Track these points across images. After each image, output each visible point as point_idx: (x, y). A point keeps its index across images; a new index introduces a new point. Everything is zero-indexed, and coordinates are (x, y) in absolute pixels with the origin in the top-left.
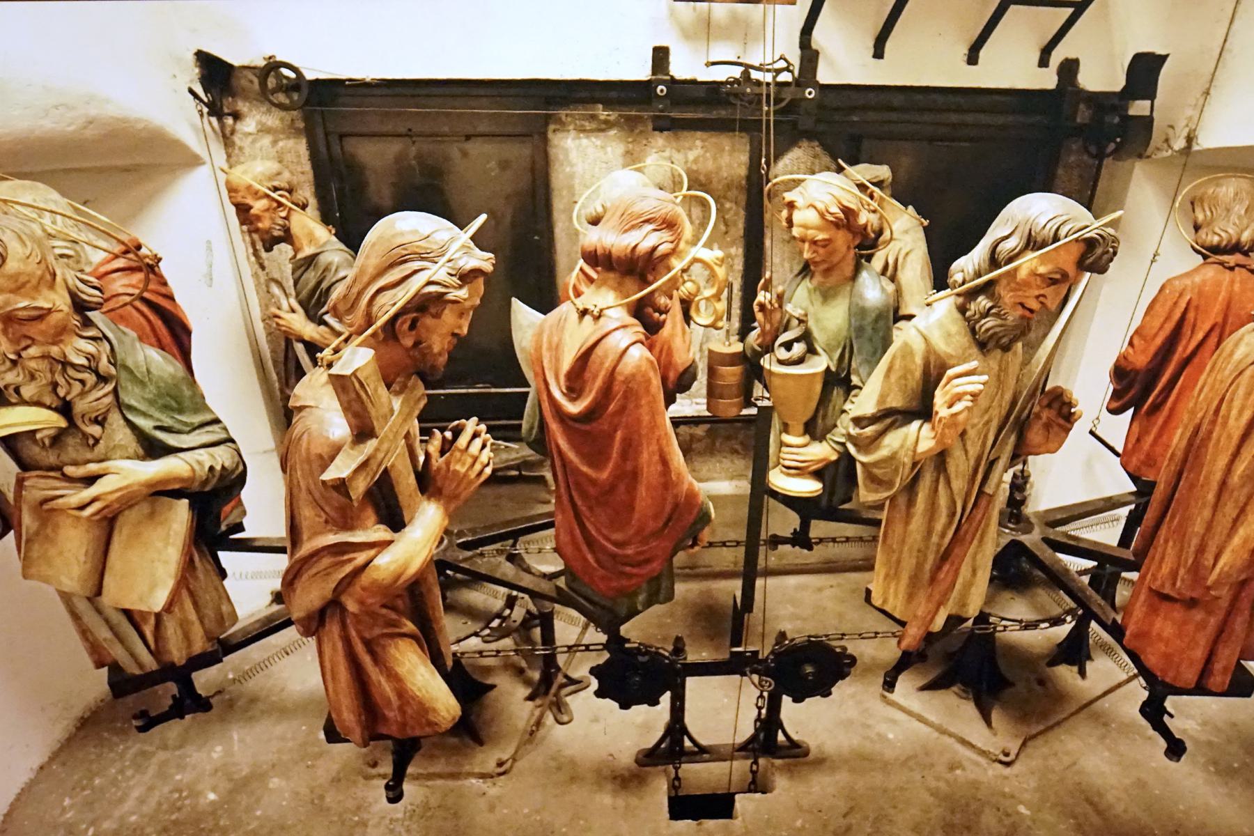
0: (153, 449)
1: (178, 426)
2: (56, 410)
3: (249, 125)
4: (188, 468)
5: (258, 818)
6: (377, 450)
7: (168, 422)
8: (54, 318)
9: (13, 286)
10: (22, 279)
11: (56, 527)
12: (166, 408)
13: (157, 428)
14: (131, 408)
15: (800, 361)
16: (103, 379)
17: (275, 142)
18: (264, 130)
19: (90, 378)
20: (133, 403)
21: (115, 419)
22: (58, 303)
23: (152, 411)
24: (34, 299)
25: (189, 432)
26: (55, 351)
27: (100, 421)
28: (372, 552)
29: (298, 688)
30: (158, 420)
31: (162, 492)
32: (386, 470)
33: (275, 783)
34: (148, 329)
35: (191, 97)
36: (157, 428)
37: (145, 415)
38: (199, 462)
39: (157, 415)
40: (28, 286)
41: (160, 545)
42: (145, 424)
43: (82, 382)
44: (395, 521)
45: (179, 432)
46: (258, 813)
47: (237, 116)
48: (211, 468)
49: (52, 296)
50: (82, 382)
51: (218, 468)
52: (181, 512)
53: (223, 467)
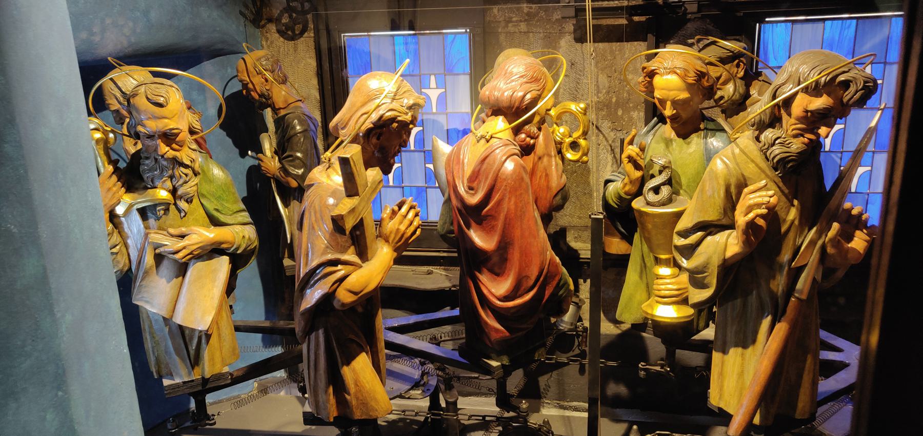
0: (215, 222)
2: (169, 191)
6: (359, 204)
14: (203, 196)
15: (669, 201)
16: (196, 174)
21: (195, 201)
27: (189, 201)
28: (350, 268)
31: (214, 251)
32: (362, 219)
42: (210, 207)
43: (186, 175)
44: (363, 254)
50: (186, 175)
52: (223, 264)
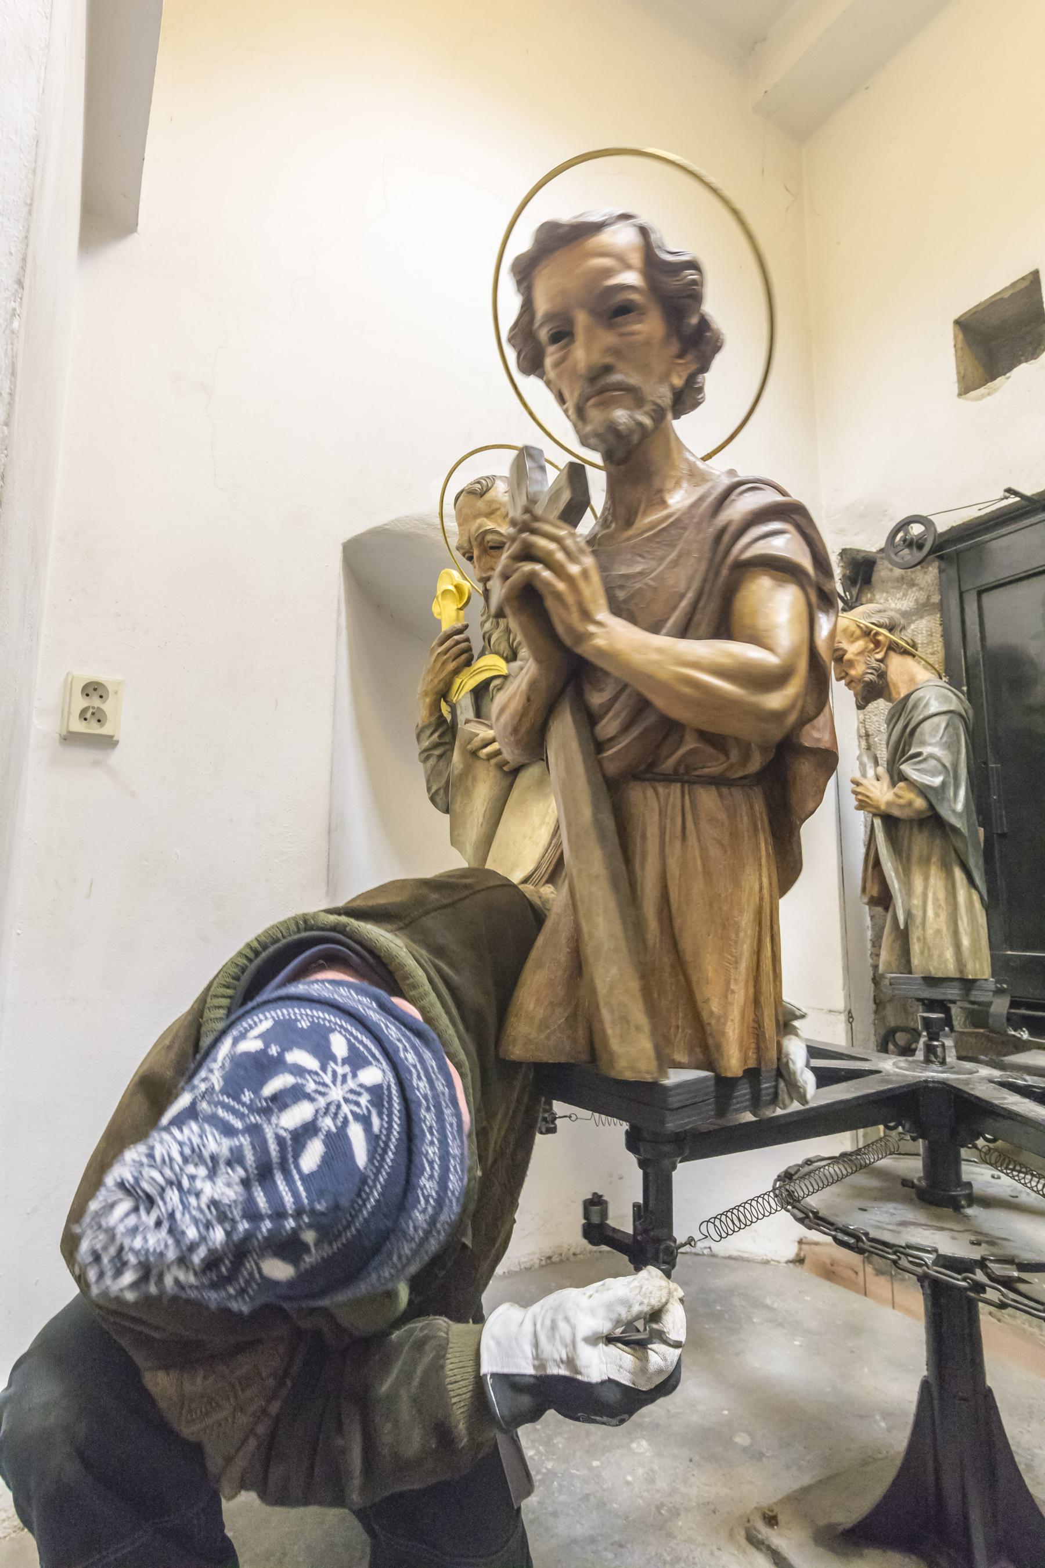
5: (590, 1468)
9: (487, 511)
10: (495, 506)
11: (474, 779)
24: (499, 525)
29: (757, 1365)
40: (498, 513)
41: (536, 820)
46: (596, 1463)
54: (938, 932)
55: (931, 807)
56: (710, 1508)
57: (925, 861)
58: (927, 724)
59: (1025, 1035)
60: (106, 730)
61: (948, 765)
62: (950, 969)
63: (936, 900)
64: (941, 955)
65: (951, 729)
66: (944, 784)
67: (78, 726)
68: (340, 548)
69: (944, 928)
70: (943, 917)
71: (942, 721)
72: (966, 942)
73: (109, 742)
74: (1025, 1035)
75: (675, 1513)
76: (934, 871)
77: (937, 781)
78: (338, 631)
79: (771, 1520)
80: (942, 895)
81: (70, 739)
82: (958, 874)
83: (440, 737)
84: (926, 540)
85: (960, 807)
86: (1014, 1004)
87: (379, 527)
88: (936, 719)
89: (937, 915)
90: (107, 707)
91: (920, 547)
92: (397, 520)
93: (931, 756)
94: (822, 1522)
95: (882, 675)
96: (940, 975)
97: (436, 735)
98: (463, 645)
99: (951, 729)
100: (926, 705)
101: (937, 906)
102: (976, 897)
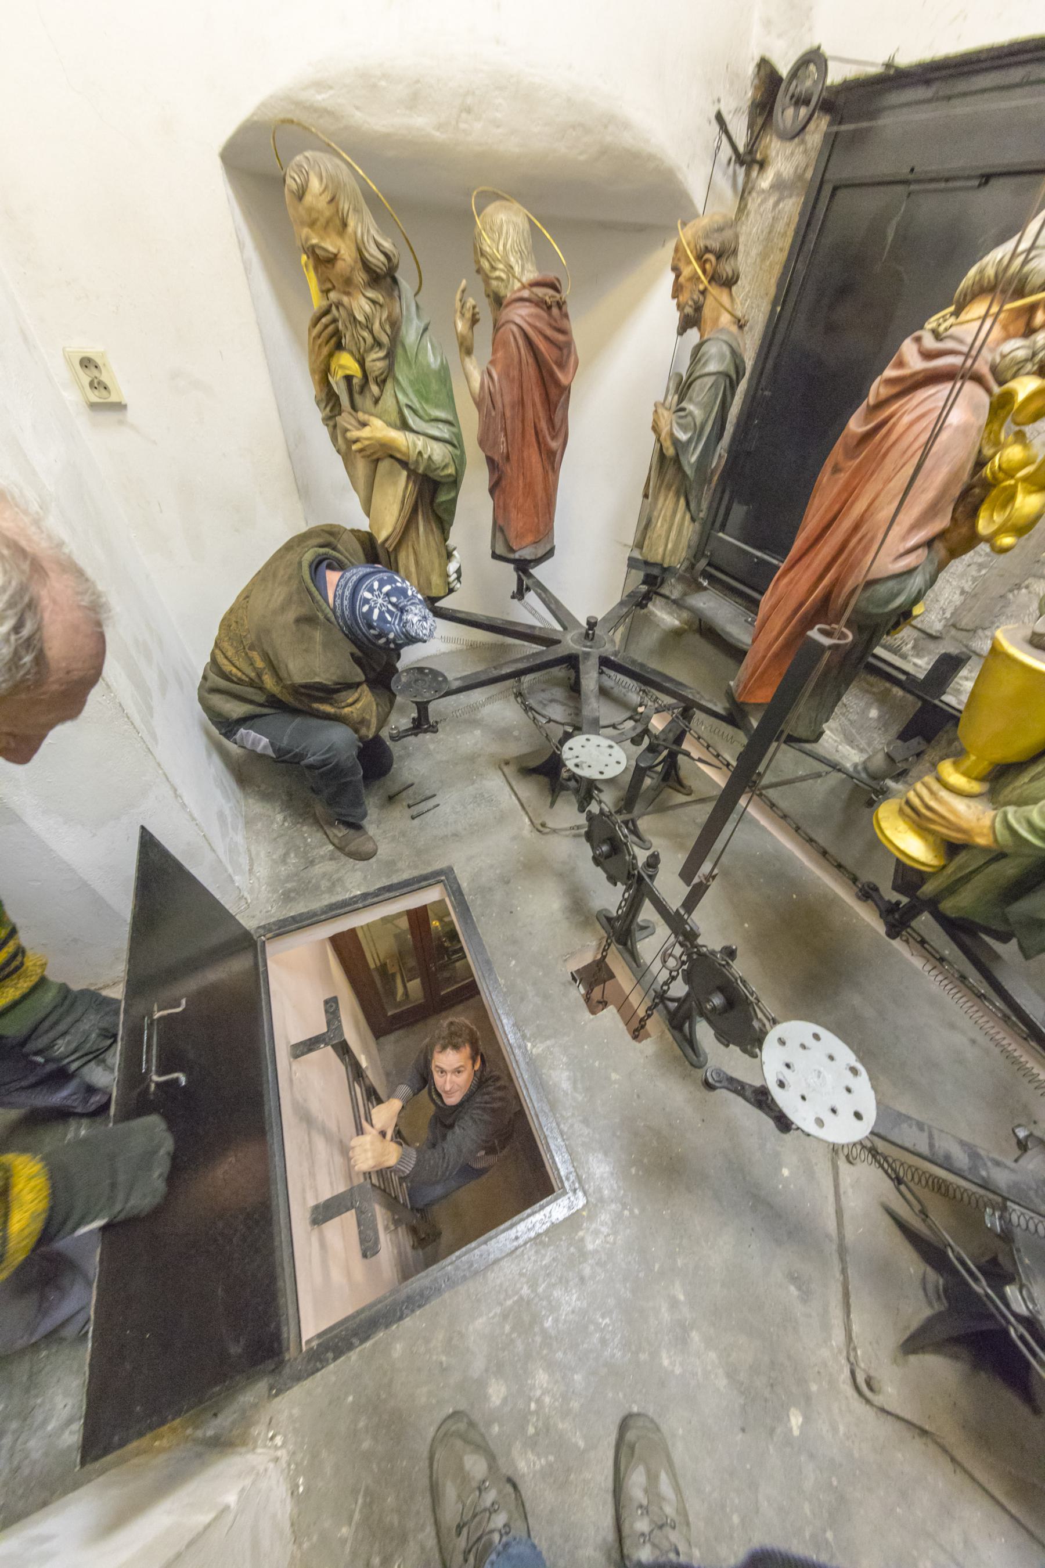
1: (421, 412)
3: (765, 181)
4: (405, 442)
7: (417, 405)
8: (340, 265)
10: (314, 215)
12: (419, 393)
13: (408, 406)
17: (776, 204)
18: (780, 186)
19: (370, 340)
20: (400, 378)
22: (342, 252)
23: (410, 391)
25: (427, 421)
26: (345, 300)
30: (411, 400)
33: (478, 732)
34: (516, 359)
35: (717, 128)
36: (408, 406)
37: (406, 394)
38: (415, 445)
39: (412, 395)
45: (420, 417)
47: (762, 165)
48: (420, 453)
49: (339, 242)
51: (426, 456)
53: (430, 457)
54: (660, 536)
55: (677, 455)
56: (492, 755)
57: (669, 488)
58: (698, 382)
59: (705, 584)
60: (114, 398)
61: (698, 424)
62: (658, 559)
63: (665, 515)
64: (657, 550)
65: (713, 390)
66: (690, 440)
67: (94, 397)
68: (218, 162)
69: (664, 534)
70: (665, 527)
71: (709, 381)
72: (670, 546)
73: (120, 407)
74: (705, 584)
75: (479, 755)
76: (671, 494)
77: (683, 437)
78: (247, 270)
79: (507, 763)
80: (669, 514)
81: (93, 406)
82: (682, 501)
83: (331, 411)
84: (812, 94)
85: (693, 459)
86: (709, 564)
87: (248, 121)
88: (706, 379)
89: (662, 526)
90: (105, 378)
91: (807, 102)
92: (263, 105)
93: (691, 414)
94: (524, 765)
95: (698, 308)
96: (652, 561)
97: (328, 409)
98: (331, 328)
99: (713, 390)
100: (705, 364)
101: (664, 520)
102: (688, 517)
